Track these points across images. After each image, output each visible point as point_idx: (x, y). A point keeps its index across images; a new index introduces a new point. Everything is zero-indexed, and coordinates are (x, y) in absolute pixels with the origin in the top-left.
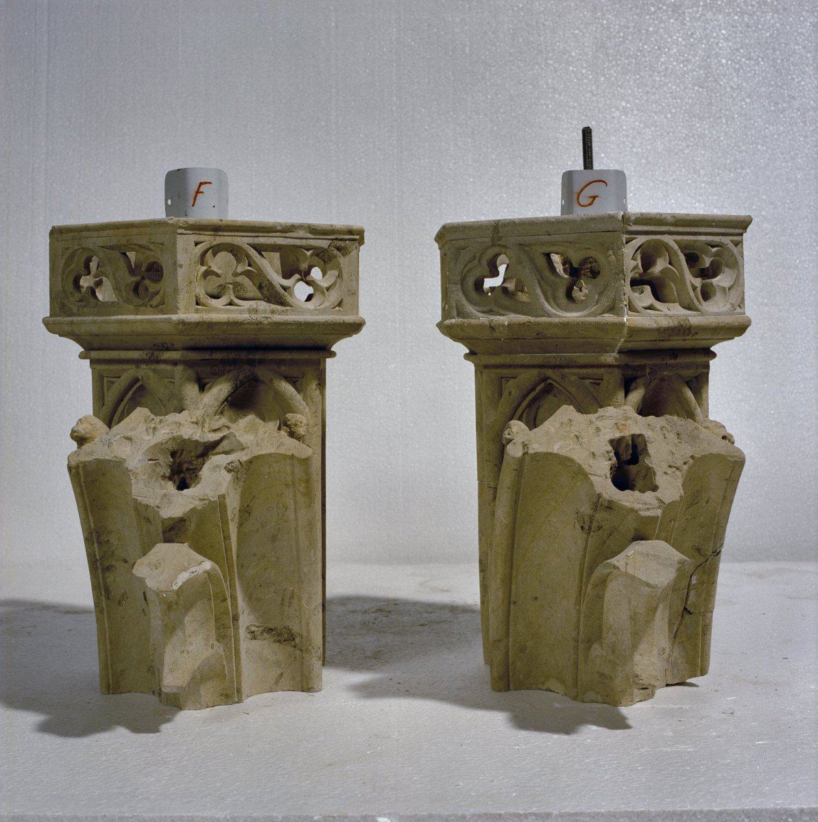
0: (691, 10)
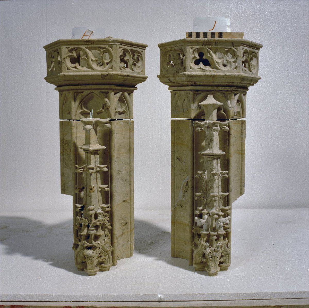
0: (256, 30)
